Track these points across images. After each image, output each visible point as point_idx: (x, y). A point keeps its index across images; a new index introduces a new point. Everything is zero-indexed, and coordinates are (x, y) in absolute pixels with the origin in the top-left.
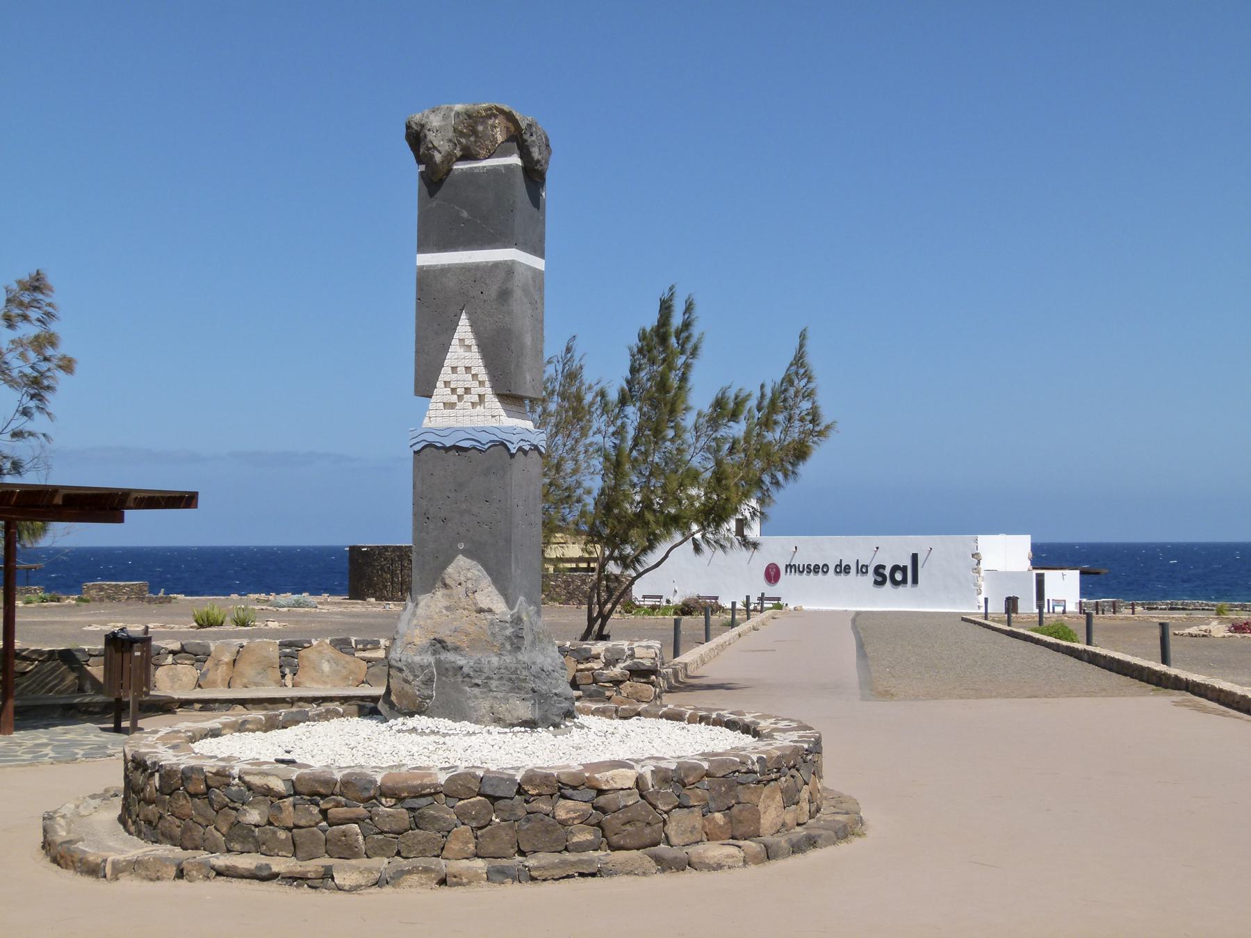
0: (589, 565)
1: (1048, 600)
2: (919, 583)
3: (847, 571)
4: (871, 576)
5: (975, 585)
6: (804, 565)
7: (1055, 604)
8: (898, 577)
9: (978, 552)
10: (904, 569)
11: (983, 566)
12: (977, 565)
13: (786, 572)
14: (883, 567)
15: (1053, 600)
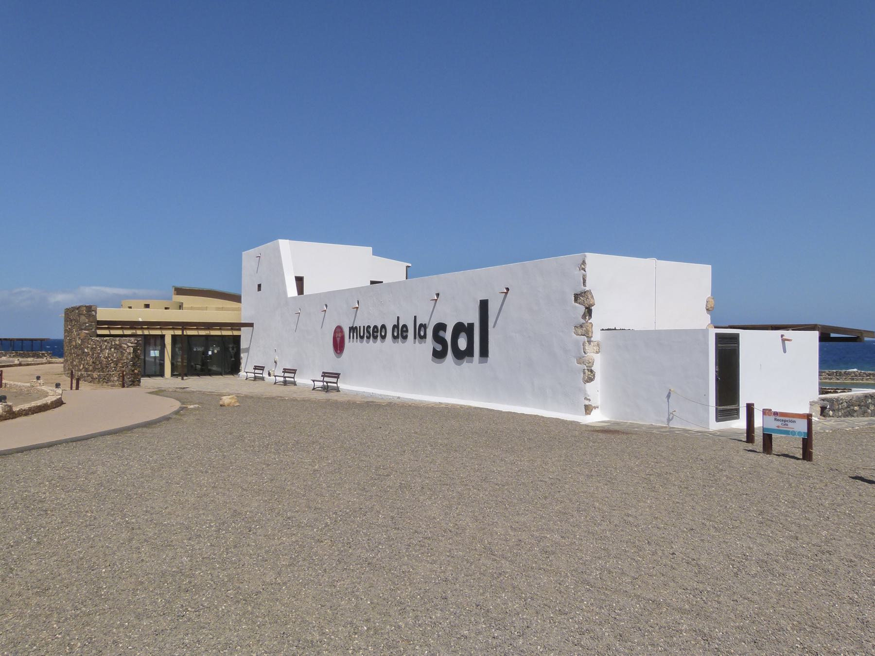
1: (750, 408)
2: (489, 356)
3: (405, 334)
4: (429, 344)
5: (580, 360)
6: (364, 327)
7: (772, 424)
8: (462, 344)
9: (587, 289)
10: (468, 330)
11: (598, 320)
12: (584, 317)
13: (350, 338)
15: (766, 412)
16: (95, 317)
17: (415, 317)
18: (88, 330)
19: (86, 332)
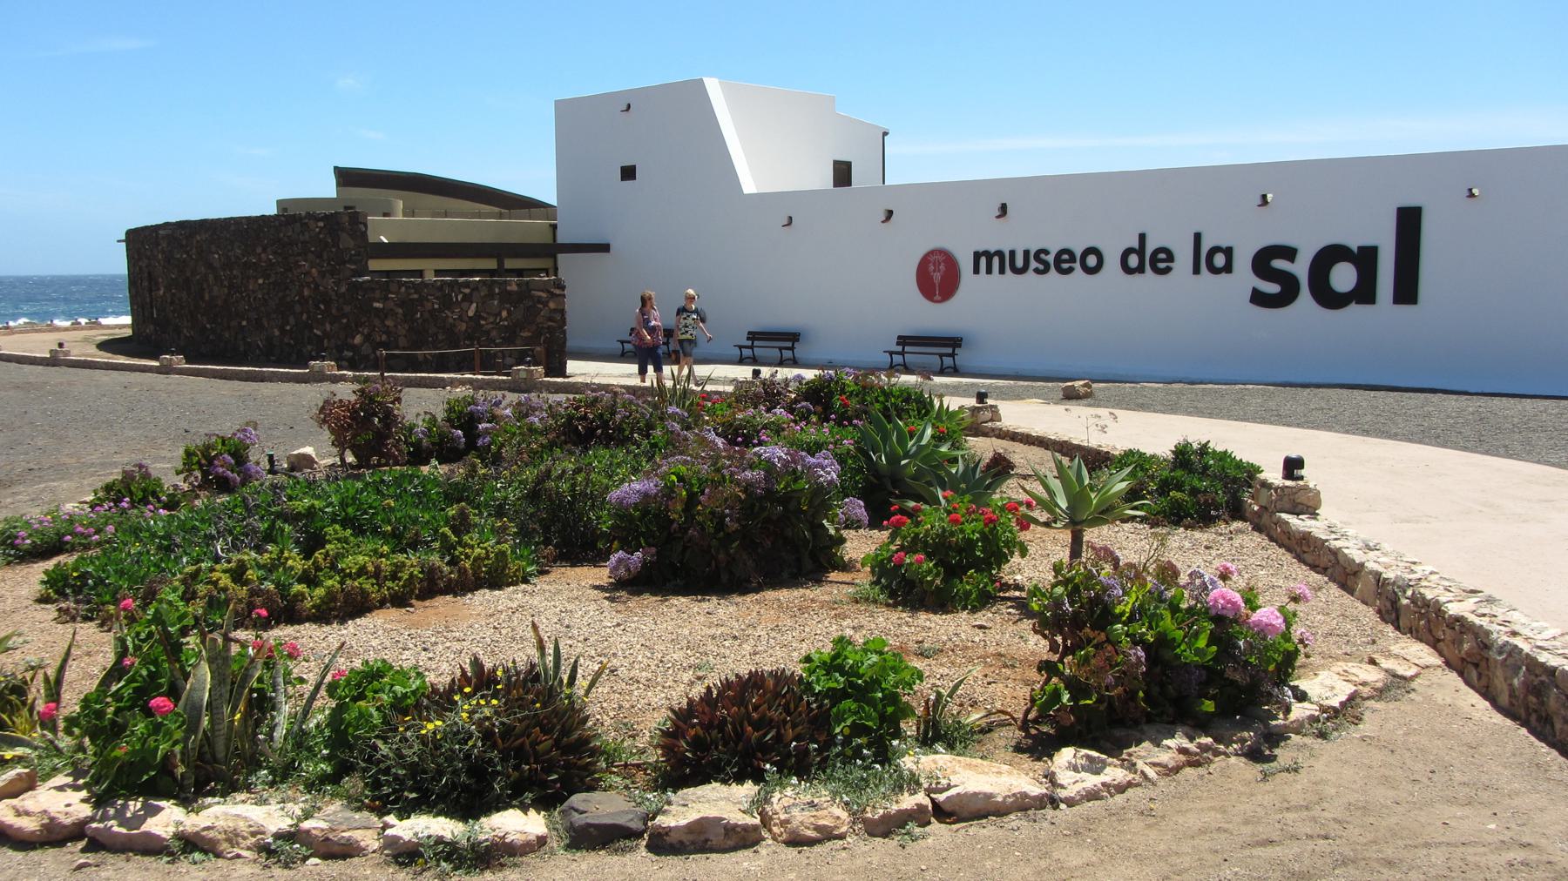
0: (501, 264)
3: (1162, 265)
4: (1244, 278)
6: (1026, 253)
8: (1343, 277)
10: (1365, 259)
13: (976, 271)
14: (1289, 253)
16: (364, 235)
17: (1198, 237)
18: (355, 264)
19: (353, 267)
